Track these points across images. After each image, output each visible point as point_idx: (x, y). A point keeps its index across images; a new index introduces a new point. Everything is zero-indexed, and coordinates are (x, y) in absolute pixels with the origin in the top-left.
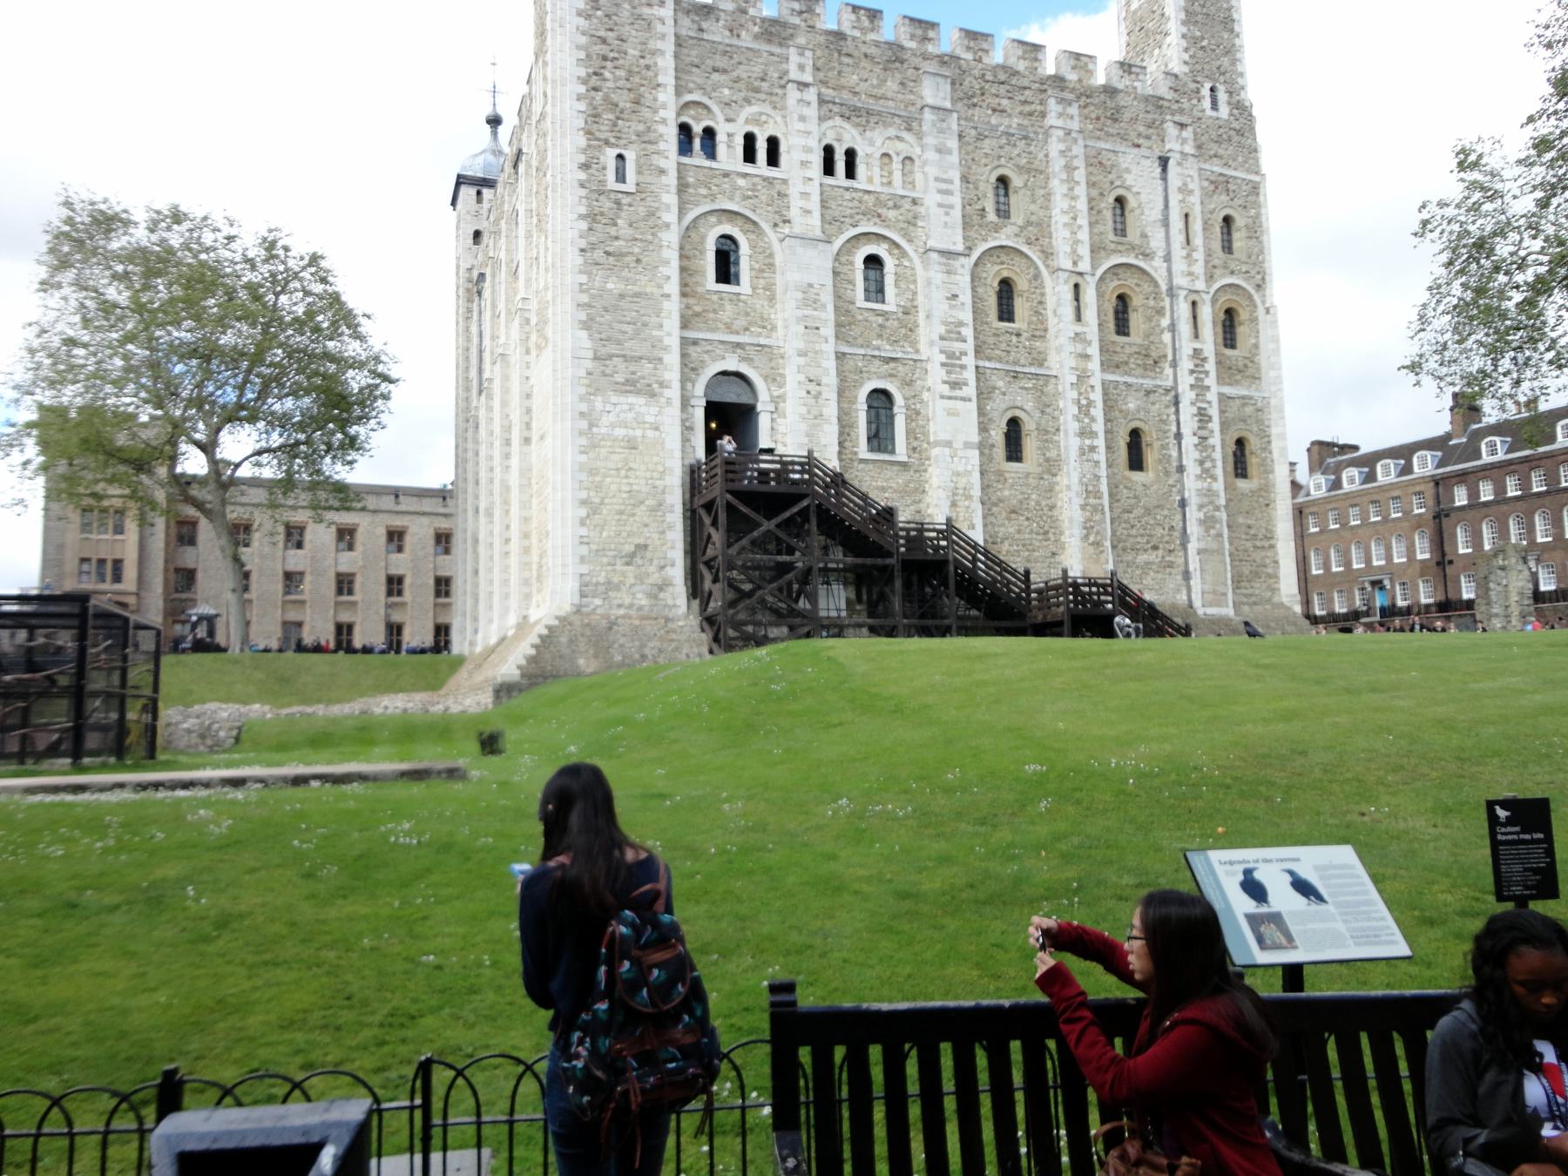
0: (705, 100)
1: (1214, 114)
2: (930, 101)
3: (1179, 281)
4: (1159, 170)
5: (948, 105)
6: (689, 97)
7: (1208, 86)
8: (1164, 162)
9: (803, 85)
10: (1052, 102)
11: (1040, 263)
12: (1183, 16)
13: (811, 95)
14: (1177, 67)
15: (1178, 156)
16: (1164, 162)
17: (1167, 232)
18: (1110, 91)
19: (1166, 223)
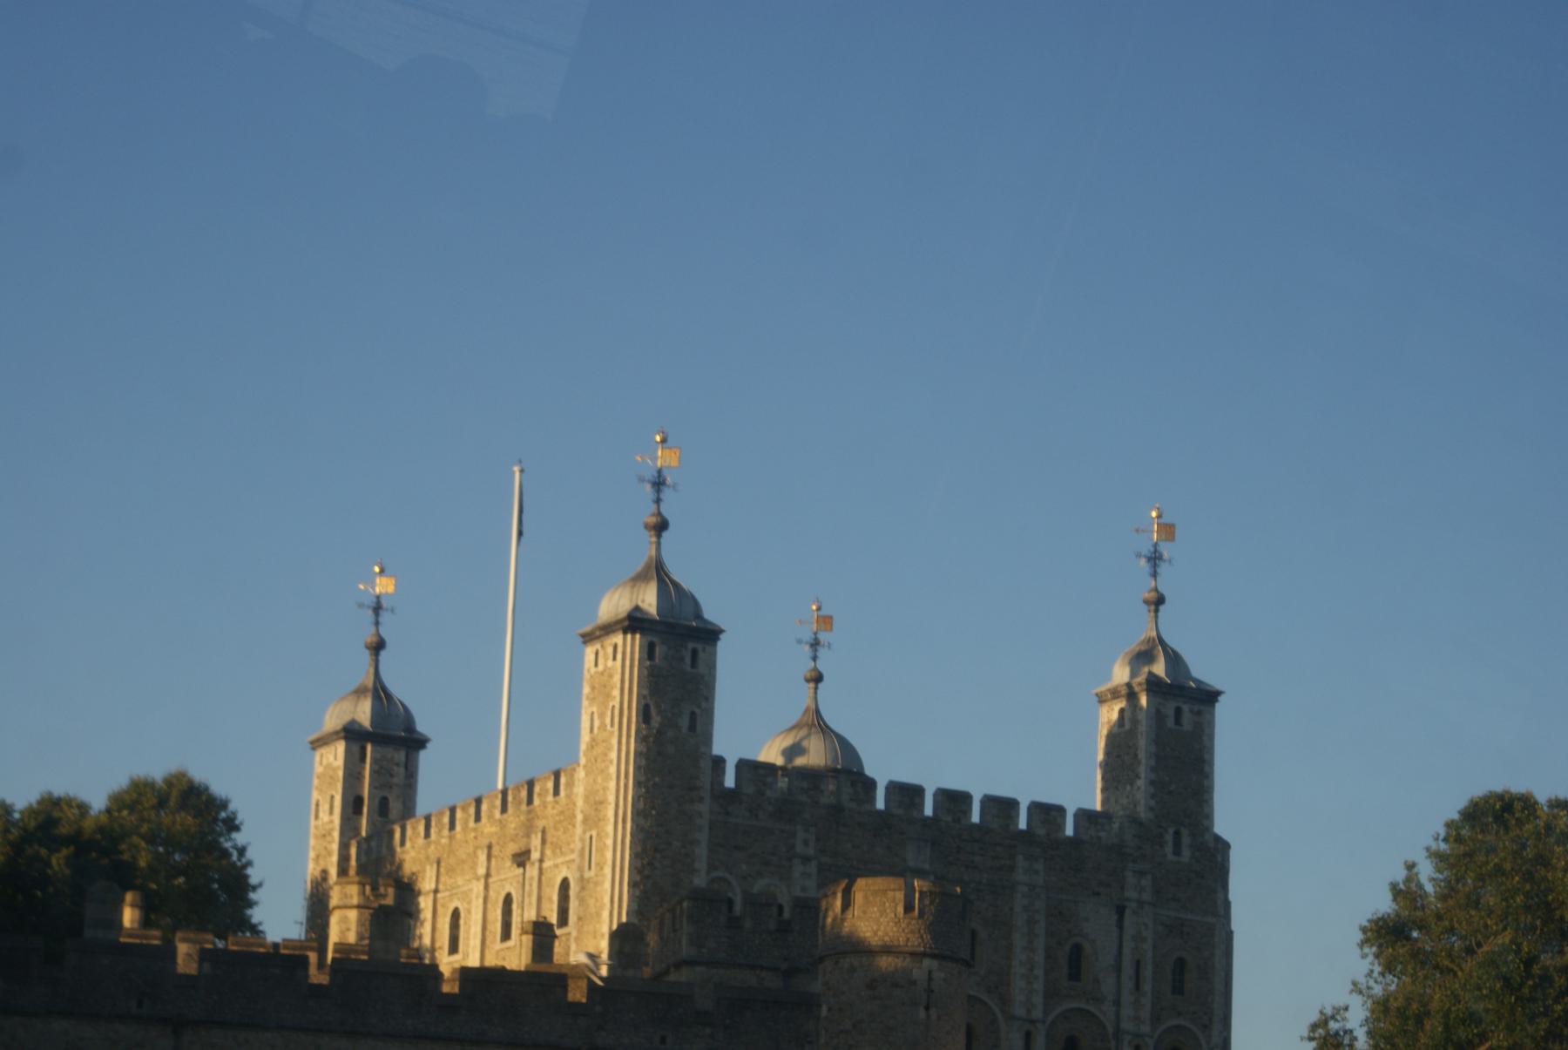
0: (728, 876)
1: (1175, 858)
2: (911, 864)
3: (1127, 1025)
4: (1115, 917)
5: (927, 866)
6: (715, 874)
7: (1171, 831)
8: (1121, 911)
9: (806, 860)
10: (1020, 858)
11: (997, 1010)
12: (1153, 763)
13: (812, 868)
14: (1143, 813)
15: (1133, 905)
16: (1121, 911)
17: (1119, 977)
18: (1075, 842)
19: (1118, 969)
